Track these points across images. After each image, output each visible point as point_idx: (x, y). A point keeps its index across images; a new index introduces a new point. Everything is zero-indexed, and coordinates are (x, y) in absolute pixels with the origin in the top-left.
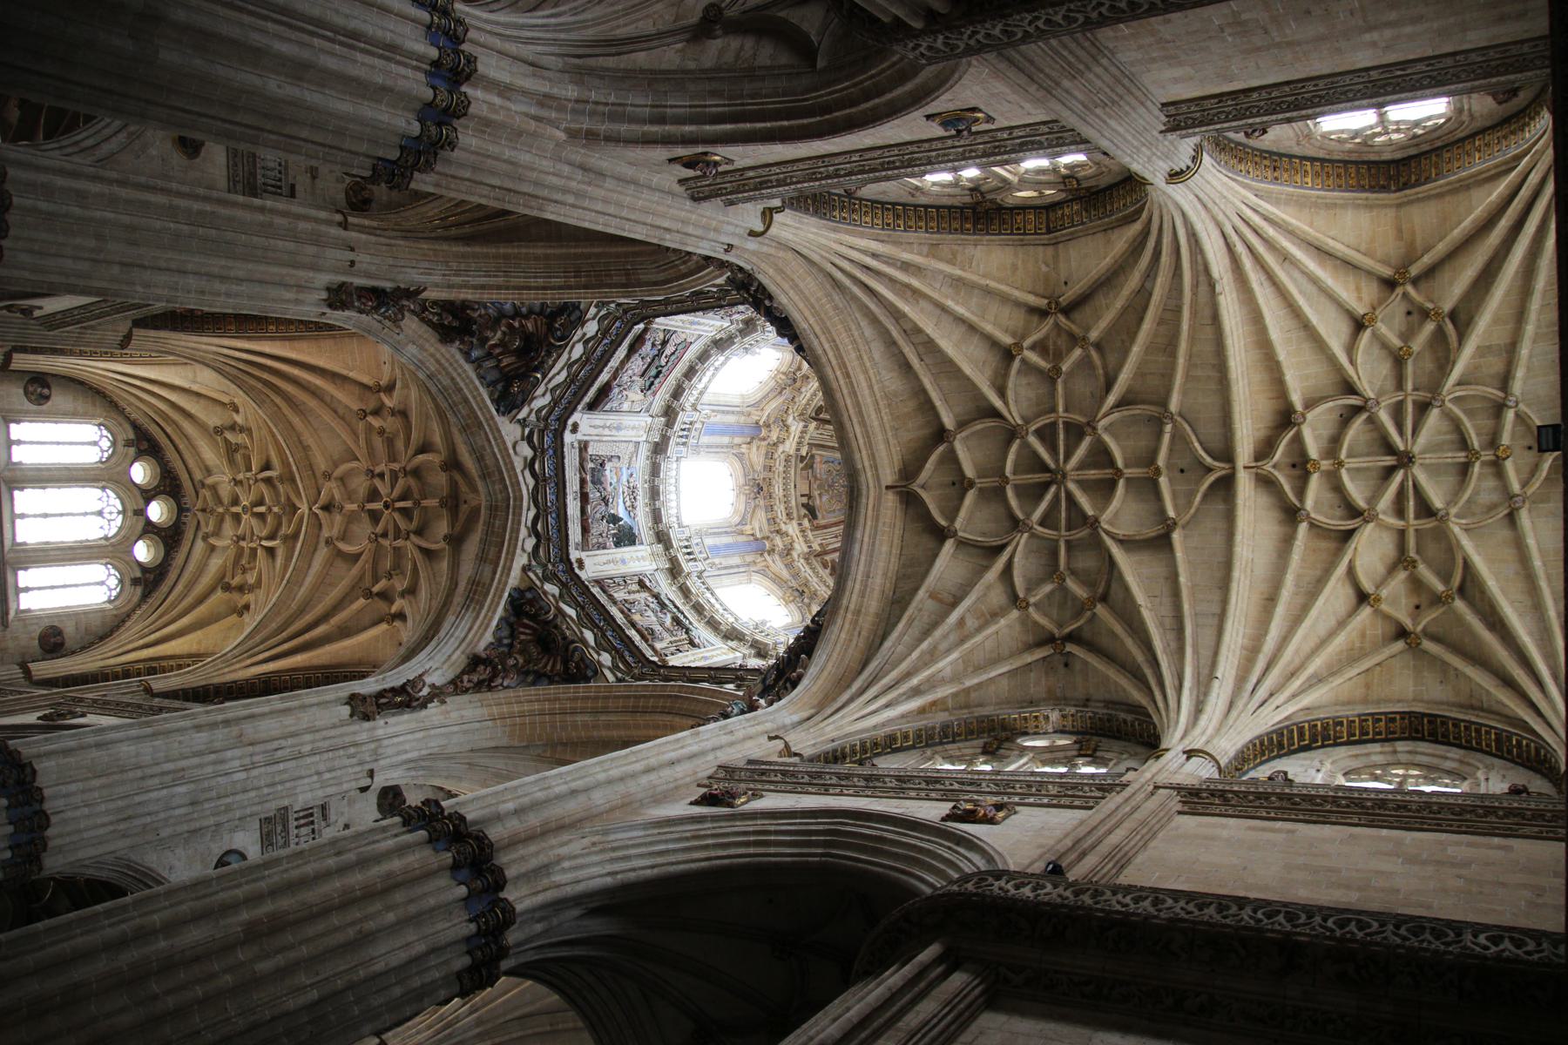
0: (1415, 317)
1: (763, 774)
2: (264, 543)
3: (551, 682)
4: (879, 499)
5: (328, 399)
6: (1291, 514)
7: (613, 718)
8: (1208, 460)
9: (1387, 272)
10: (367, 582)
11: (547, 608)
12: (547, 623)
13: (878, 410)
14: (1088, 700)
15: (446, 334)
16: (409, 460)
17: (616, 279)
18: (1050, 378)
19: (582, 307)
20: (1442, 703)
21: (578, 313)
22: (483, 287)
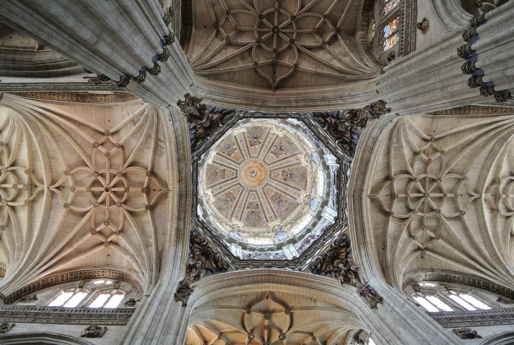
1: (451, 319)
2: (10, 204)
3: (212, 272)
4: (366, 200)
5: (73, 135)
6: (494, 211)
8: (473, 194)
10: (93, 226)
11: (203, 239)
12: (204, 246)
13: (375, 169)
14: (432, 269)
15: (191, 118)
17: (258, 103)
18: (427, 164)
21: (233, 114)
22: (214, 100)
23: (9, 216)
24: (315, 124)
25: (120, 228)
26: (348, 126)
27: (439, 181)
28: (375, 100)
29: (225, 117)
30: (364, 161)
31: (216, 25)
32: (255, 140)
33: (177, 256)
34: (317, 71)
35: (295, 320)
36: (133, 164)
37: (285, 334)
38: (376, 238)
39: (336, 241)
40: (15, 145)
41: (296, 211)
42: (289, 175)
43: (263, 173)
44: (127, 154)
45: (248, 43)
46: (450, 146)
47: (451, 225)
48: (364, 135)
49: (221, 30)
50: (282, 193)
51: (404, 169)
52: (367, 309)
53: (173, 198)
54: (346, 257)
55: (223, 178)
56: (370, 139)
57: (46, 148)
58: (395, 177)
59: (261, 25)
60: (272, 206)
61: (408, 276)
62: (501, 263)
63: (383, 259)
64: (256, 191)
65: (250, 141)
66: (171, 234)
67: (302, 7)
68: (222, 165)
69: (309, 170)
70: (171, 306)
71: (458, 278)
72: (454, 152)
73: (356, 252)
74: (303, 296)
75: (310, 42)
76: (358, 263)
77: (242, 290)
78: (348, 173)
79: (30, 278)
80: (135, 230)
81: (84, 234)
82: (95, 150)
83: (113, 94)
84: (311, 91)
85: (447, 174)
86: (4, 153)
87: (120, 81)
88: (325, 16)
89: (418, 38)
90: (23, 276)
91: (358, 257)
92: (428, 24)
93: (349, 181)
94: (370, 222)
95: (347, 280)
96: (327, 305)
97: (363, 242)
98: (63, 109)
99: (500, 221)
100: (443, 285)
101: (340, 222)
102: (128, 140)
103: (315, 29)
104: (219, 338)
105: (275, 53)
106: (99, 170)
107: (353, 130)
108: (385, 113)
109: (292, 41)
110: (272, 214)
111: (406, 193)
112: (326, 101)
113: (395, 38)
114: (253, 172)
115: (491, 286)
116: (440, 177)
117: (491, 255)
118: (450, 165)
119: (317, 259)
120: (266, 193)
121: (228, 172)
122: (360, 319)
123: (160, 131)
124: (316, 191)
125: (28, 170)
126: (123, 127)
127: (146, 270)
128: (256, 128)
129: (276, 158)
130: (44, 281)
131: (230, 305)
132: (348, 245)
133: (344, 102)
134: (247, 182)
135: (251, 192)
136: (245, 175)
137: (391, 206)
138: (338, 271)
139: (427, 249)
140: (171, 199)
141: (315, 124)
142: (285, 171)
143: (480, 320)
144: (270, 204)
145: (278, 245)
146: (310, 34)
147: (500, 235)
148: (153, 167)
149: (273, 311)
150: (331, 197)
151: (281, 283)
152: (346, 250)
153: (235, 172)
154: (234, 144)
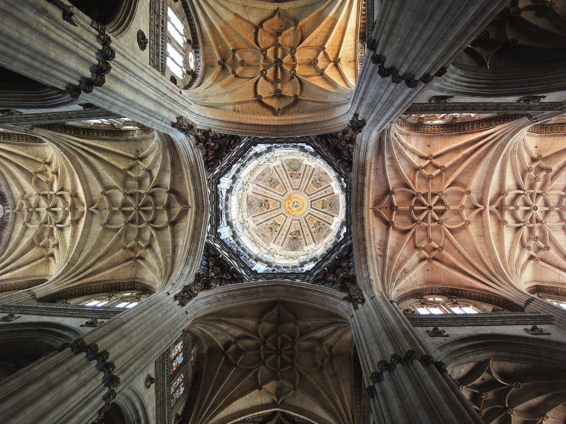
0: (47, 246)
1: (108, 115)
2: (522, 192)
3: (331, 135)
4: (192, 203)
5: (461, 258)
6: (75, 195)
7: (299, 122)
8: (95, 211)
9: (51, 258)
11: (340, 164)
12: (339, 158)
13: (186, 233)
14: (128, 141)
15: (352, 280)
16: (415, 226)
19: (312, 281)
20: (37, 146)
21: (315, 279)
22: (333, 296)
23: (523, 180)
24: (241, 270)
25: (418, 173)
26: (211, 272)
27: (127, 222)
28: (189, 304)
29: (322, 277)
30: (195, 241)
31: (332, 356)
32: (295, 236)
33: (364, 152)
34: (240, 320)
35: (252, 90)
36: (406, 232)
37: (261, 76)
38: (181, 170)
39: (218, 166)
40: (516, 248)
41: (255, 175)
42: (263, 205)
43: (287, 206)
44: (411, 241)
45: (303, 341)
46: (118, 254)
47: (113, 182)
48: (196, 266)
49: (327, 353)
50: (269, 188)
51: (159, 232)
52: (186, 114)
53: (368, 202)
54: (207, 152)
55: (323, 201)
56: (191, 263)
57: (487, 246)
58: (166, 225)
59: (292, 357)
60: (277, 176)
61: (150, 135)
62: (65, 152)
63: (174, 153)
64: (293, 189)
65: (300, 235)
66: (370, 170)
67: (256, 373)
68: (325, 213)
69: (245, 214)
70: (369, 118)
71: (103, 135)
72: (115, 248)
73: (199, 158)
74: (246, 113)
75: (248, 342)
76: (196, 149)
77: (303, 118)
78: (209, 227)
79: (503, 130)
80: (403, 172)
81: (452, 166)
82: (442, 244)
83: (424, 295)
84: (245, 302)
85: (119, 229)
86: (526, 239)
87: (413, 360)
88: (236, 366)
89: (154, 368)
90: (510, 131)
91: (197, 154)
92: (146, 384)
93: (208, 220)
94: (187, 185)
95: (206, 133)
96: (223, 107)
97: (193, 167)
98: (471, 283)
99: (69, 186)
100: (117, 128)
101: (215, 181)
102: (411, 254)
103: (244, 354)
104: (323, 70)
105: (279, 333)
106: (438, 226)
107: (206, 269)
108: (179, 294)
109: (264, 343)
110: (278, 169)
111: (156, 211)
112: (232, 295)
113: (173, 355)
114: (296, 206)
115: (73, 132)
116: (126, 226)
117: (74, 158)
118: (117, 236)
119: (234, 148)
120: (284, 188)
121: (319, 207)
122: (190, 102)
123: (380, 265)
124: (238, 197)
125: (504, 224)
126: (416, 265)
127: (393, 139)
128: (294, 249)
129: (276, 219)
130: (490, 125)
131: (313, 103)
132: (206, 163)
133: (216, 297)
134: (301, 197)
135: (298, 188)
136: (303, 203)
137: (169, 199)
138: (214, 139)
139: (133, 159)
140: (371, 201)
141: (241, 270)
142: (267, 209)
143: (81, 115)
144: (280, 178)
145: (271, 151)
146: (248, 349)
147: (68, 176)
148: (388, 230)
149: (273, 97)
150: (224, 198)
151: (266, 126)
152: (208, 158)
153: (312, 207)
154: (314, 232)
